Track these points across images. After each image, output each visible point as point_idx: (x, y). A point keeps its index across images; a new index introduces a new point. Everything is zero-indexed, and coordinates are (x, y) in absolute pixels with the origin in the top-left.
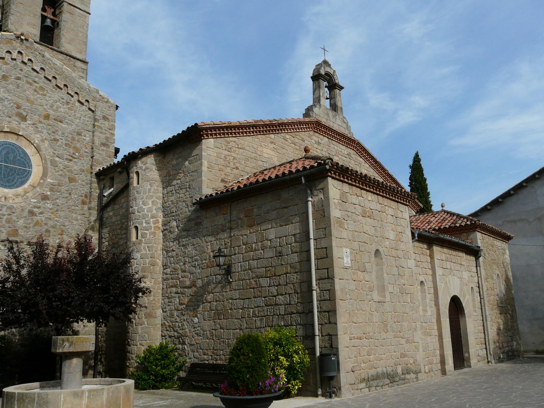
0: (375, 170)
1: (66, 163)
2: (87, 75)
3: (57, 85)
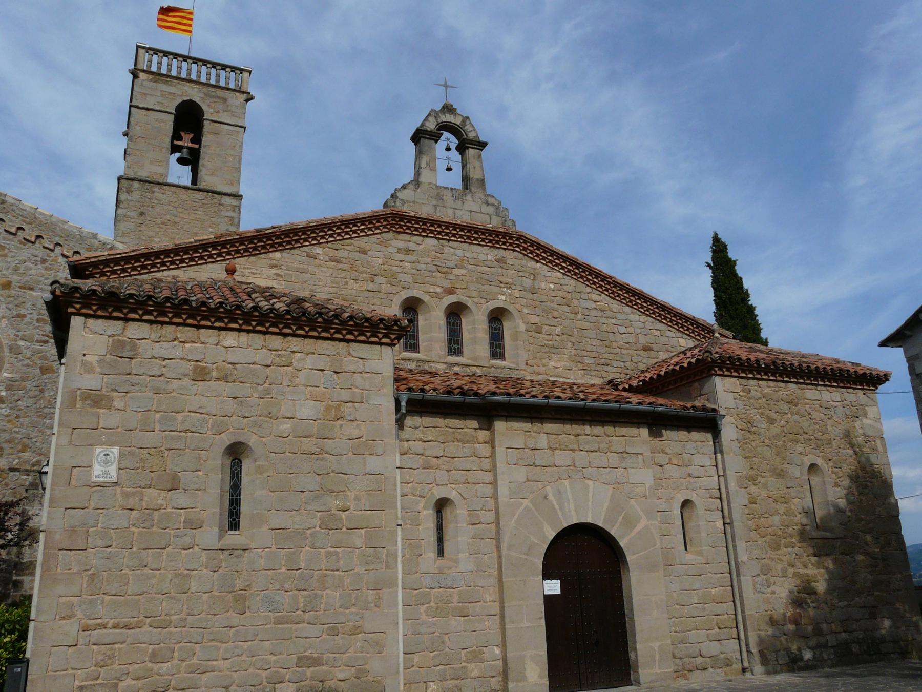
0: (582, 280)
1: (38, 347)
2: (240, 213)
3: (25, 239)
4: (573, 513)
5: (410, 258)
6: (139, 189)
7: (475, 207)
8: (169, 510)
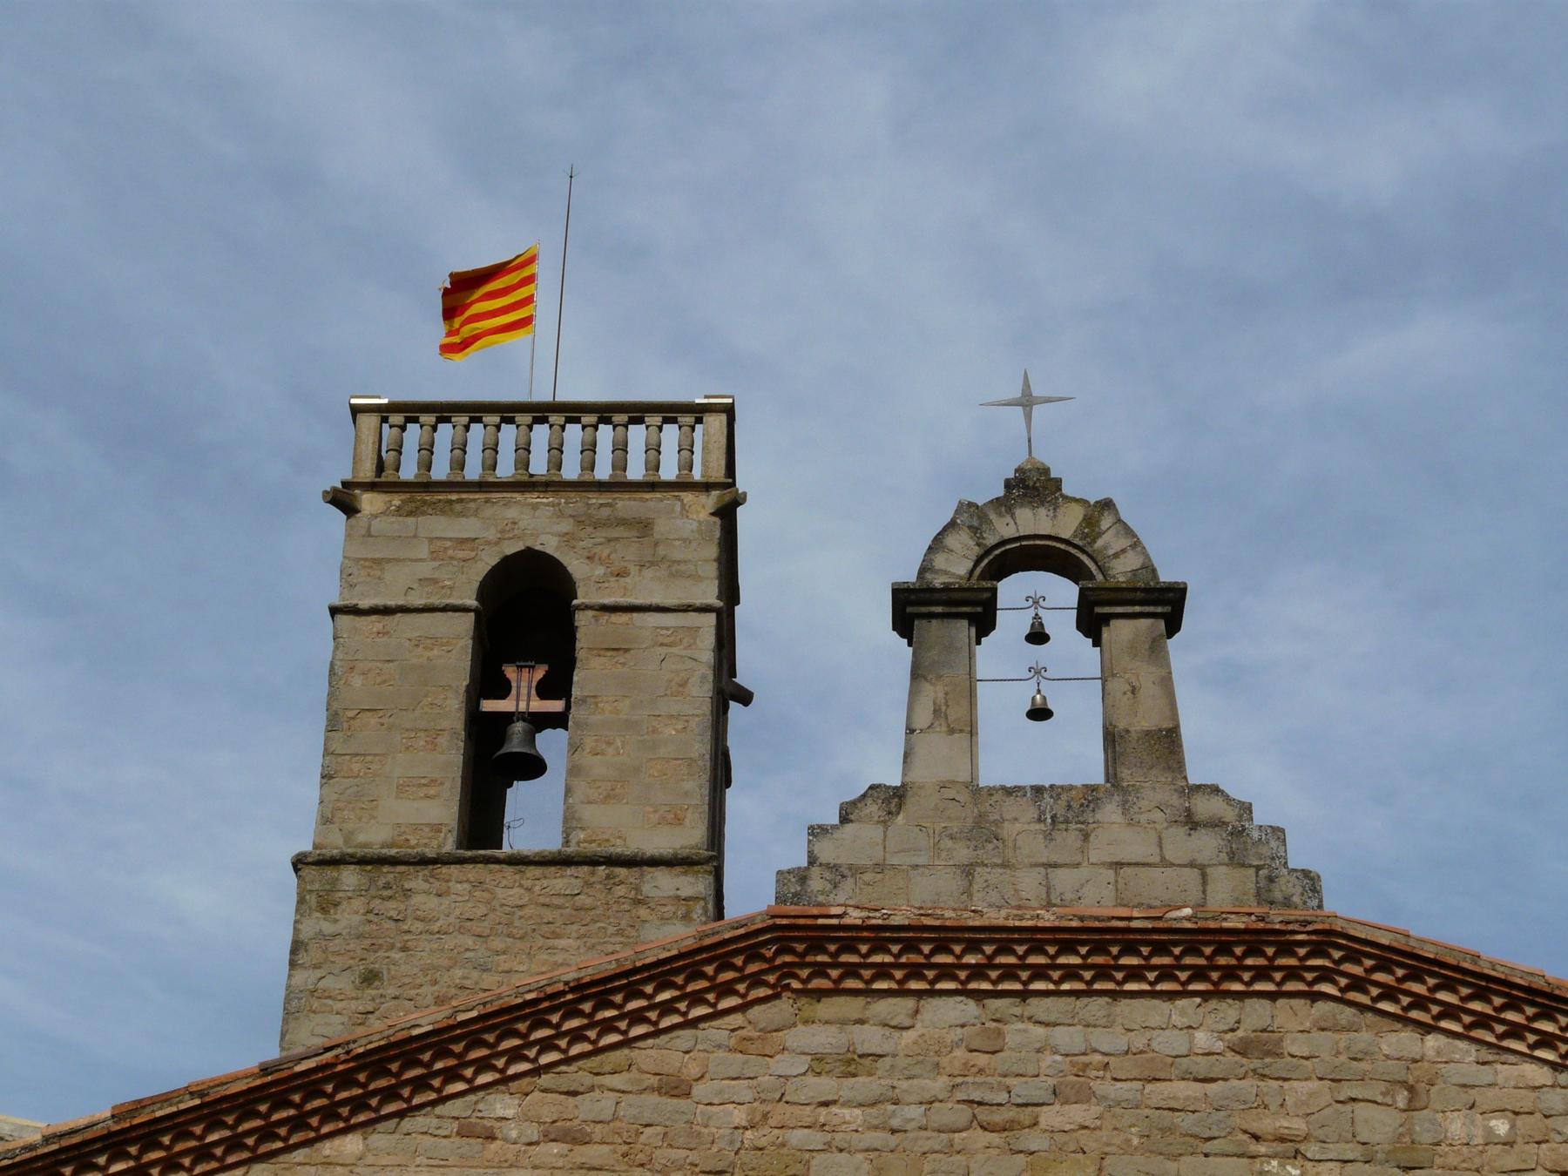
5: (864, 1086)
6: (360, 892)
7: (1137, 847)
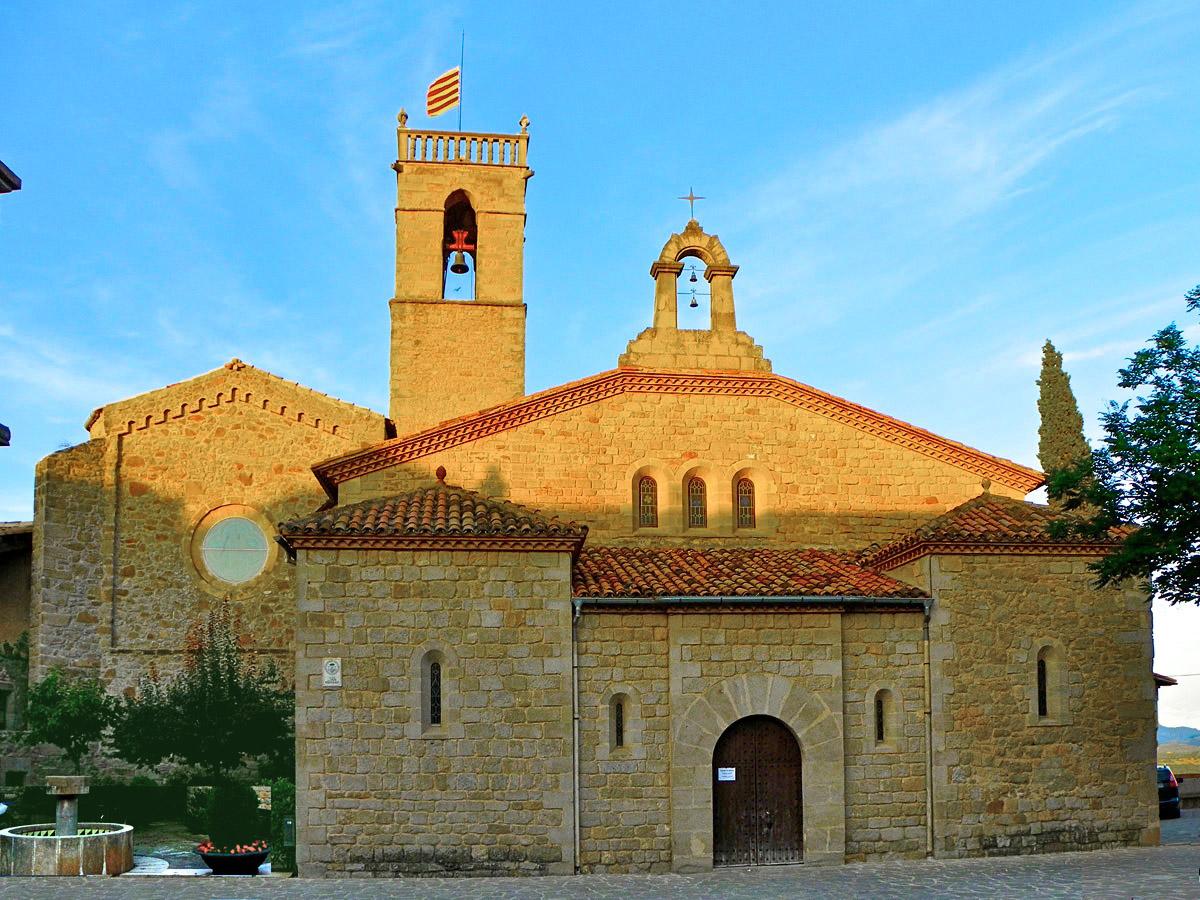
4: (749, 706)
8: (383, 708)
